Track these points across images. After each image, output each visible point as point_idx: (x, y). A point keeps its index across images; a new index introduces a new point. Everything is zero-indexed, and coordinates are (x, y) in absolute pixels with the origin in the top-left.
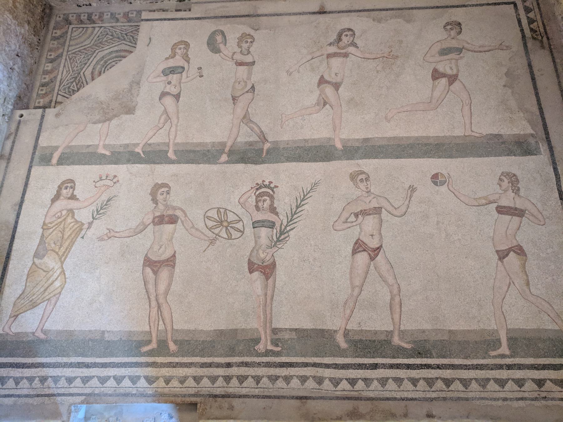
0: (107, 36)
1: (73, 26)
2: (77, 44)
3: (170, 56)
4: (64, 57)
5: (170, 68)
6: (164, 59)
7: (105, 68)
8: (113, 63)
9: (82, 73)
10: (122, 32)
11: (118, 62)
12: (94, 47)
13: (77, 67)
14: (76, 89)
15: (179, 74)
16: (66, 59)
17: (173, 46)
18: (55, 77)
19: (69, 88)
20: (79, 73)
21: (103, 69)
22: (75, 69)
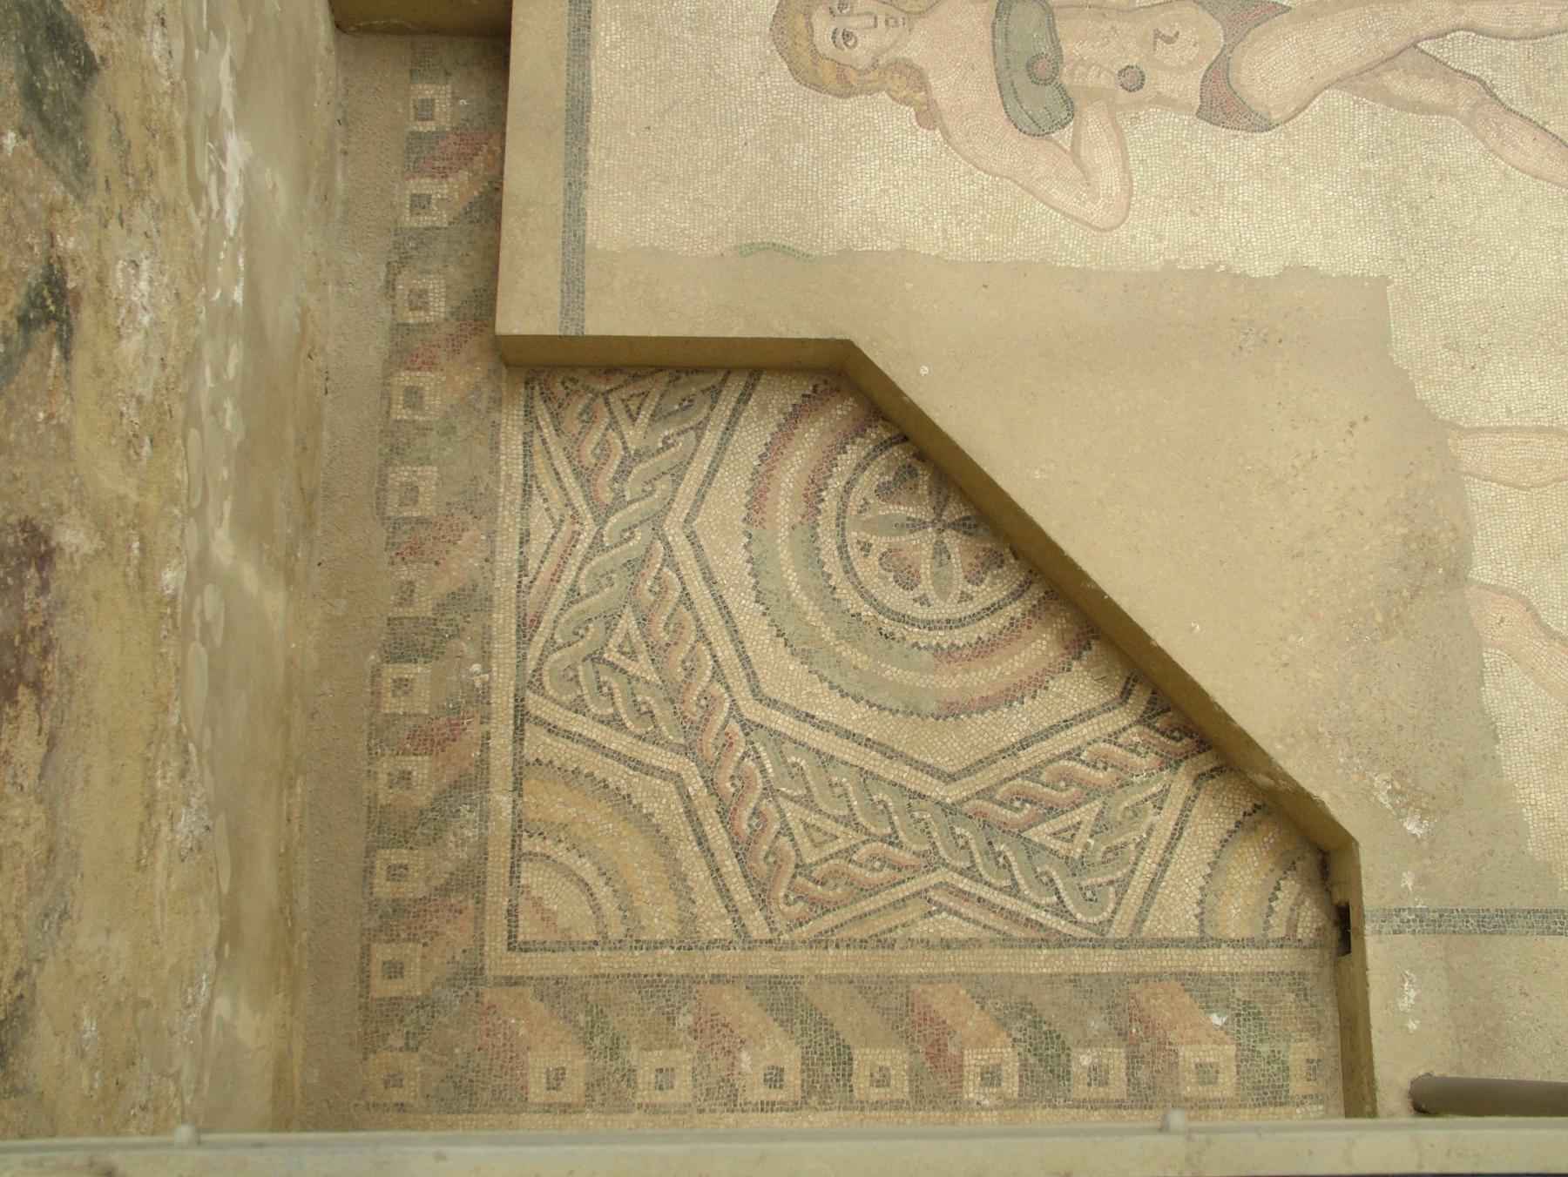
0: (612, 655)
1: (496, 945)
2: (678, 881)
3: (906, 101)
4: (797, 962)
5: (1006, 89)
6: (927, 141)
7: (913, 622)
8: (867, 569)
9: (952, 793)
10: (581, 548)
11: (852, 535)
12: (709, 739)
13: (892, 840)
14: (1086, 814)
15: (1062, 29)
16: (819, 942)
17: (818, 87)
18: (980, 989)
19: (1075, 867)
20: (950, 810)
21: (914, 634)
22: (905, 857)
